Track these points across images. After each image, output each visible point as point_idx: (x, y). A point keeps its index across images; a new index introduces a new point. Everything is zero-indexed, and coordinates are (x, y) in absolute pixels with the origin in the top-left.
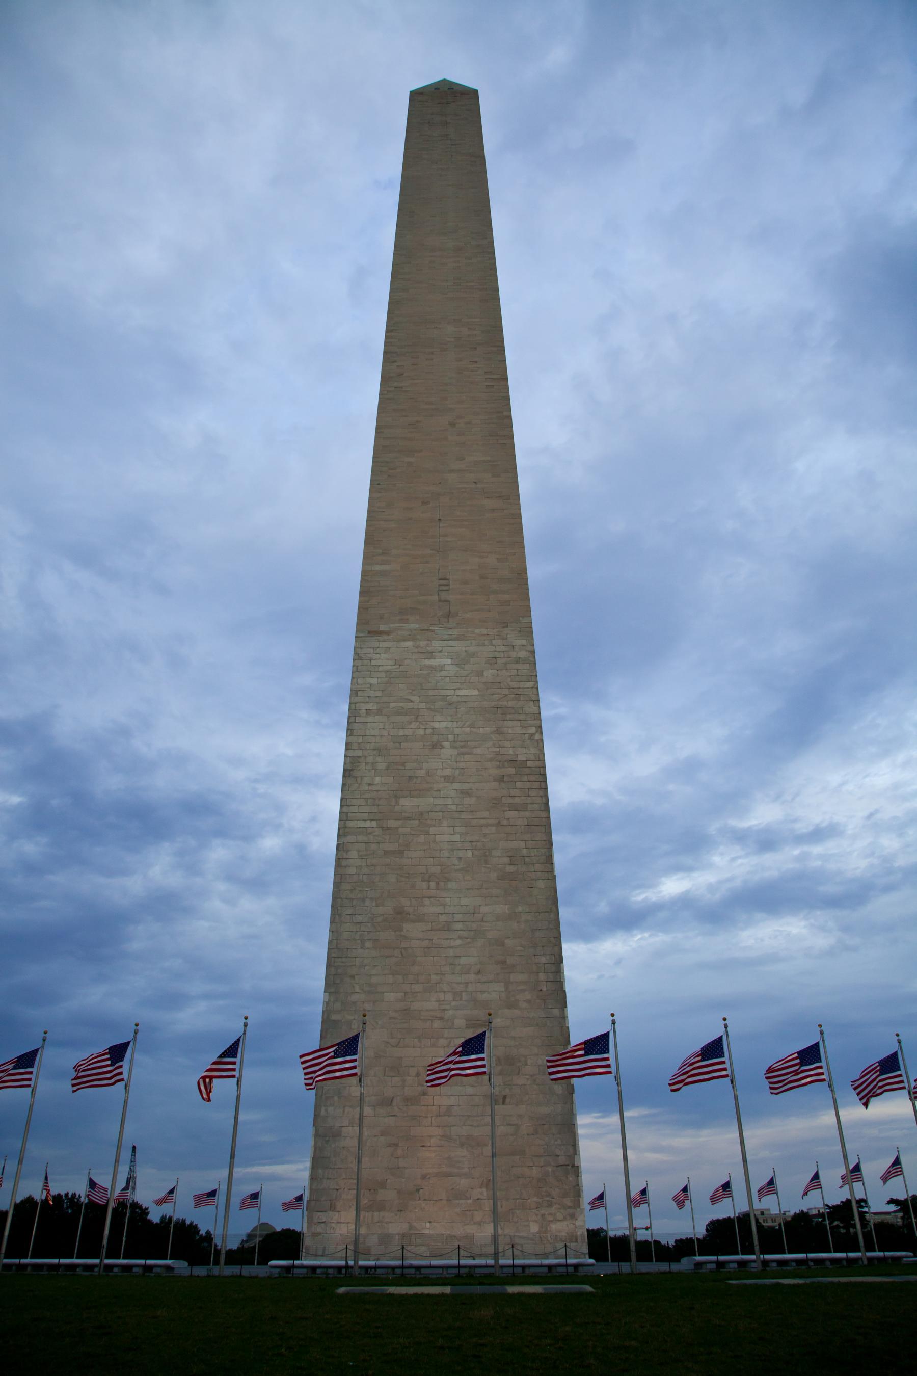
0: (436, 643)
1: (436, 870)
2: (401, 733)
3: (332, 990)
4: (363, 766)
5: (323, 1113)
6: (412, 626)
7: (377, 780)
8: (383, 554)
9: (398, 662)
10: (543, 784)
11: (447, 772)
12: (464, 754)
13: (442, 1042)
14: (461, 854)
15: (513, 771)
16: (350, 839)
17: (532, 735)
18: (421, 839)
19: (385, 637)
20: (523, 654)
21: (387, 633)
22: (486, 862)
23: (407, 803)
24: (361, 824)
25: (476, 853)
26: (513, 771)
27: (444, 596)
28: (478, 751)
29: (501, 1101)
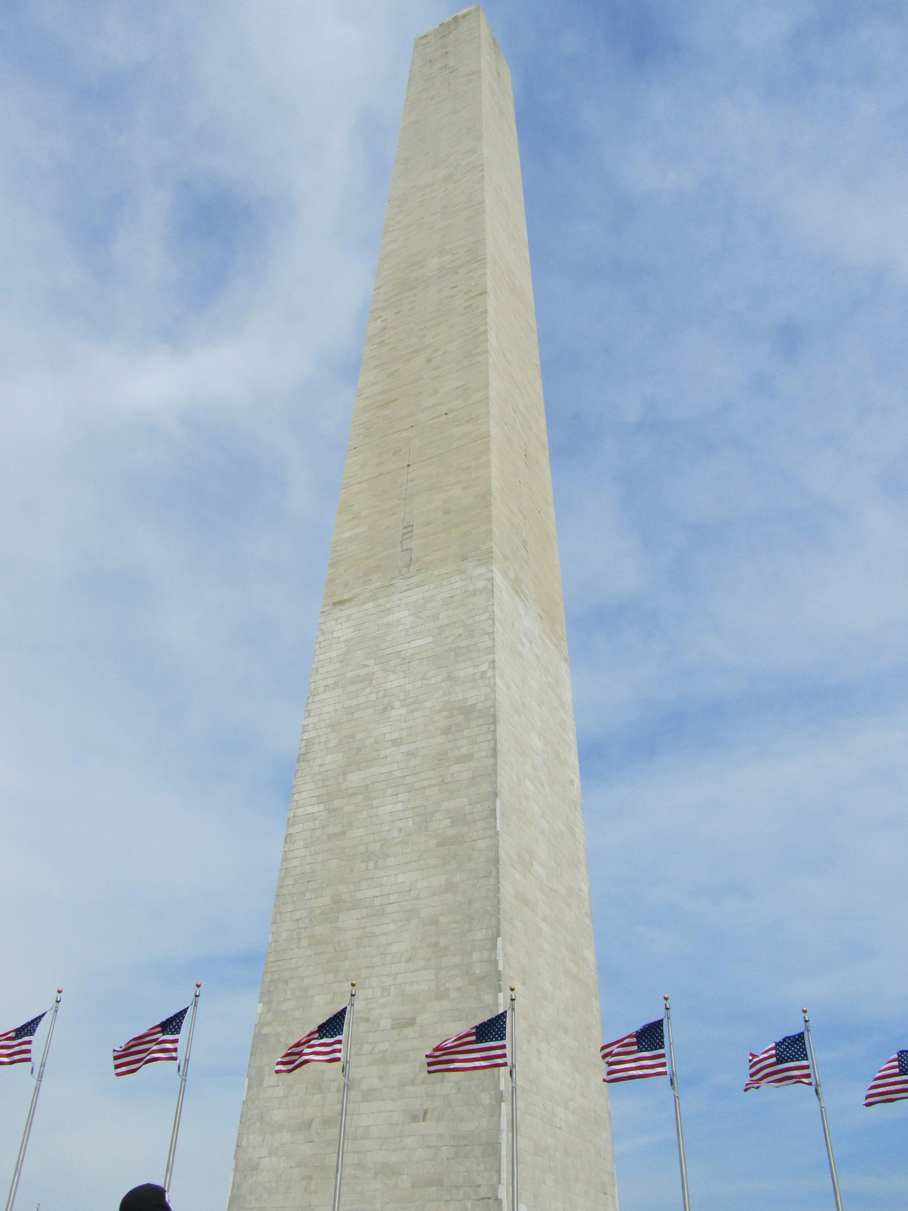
2: (355, 702)
3: (266, 999)
5: (244, 1143)
6: (374, 586)
7: (328, 758)
10: (492, 726)
11: (396, 735)
12: (413, 711)
13: (367, 1048)
14: (401, 824)
15: (461, 718)
17: (484, 672)
18: (364, 815)
19: (348, 605)
21: (350, 600)
22: (426, 830)
23: (355, 778)
24: (310, 809)
25: (417, 819)
27: (407, 544)
28: (428, 704)
29: (421, 1117)
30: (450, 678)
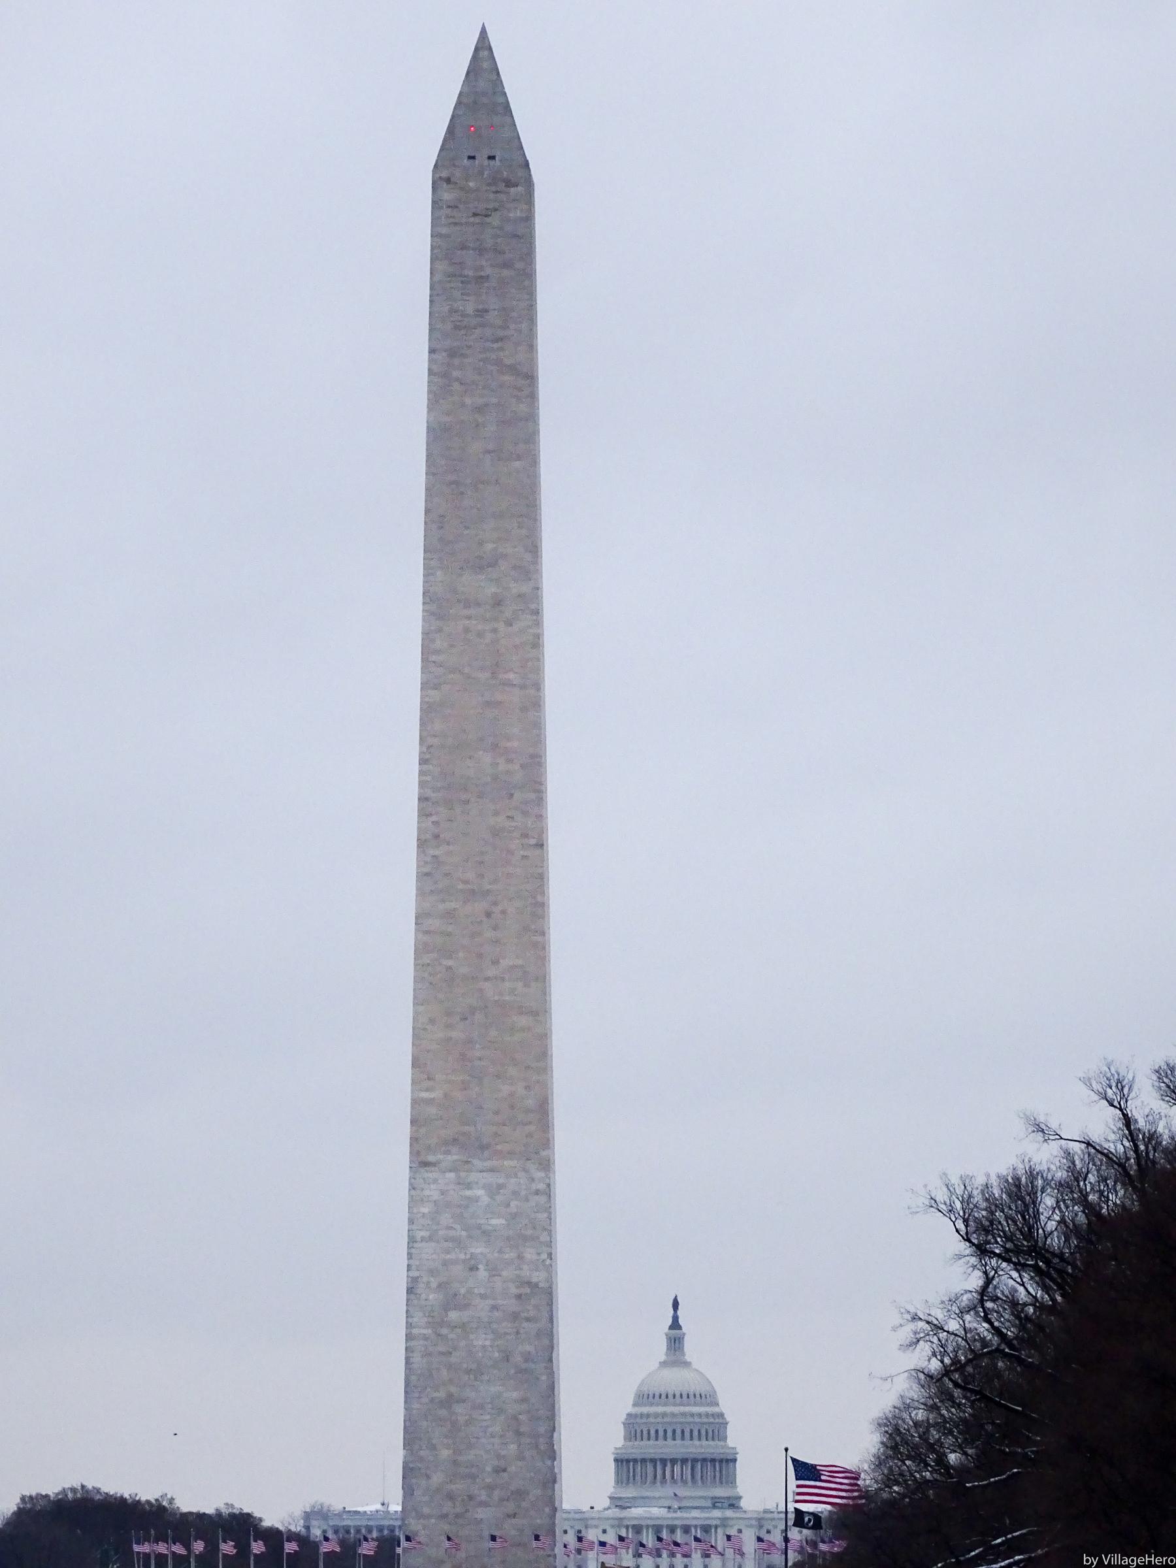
0: (473, 1177)
1: (474, 1366)
4: (421, 1285)
6: (455, 1157)
8: (429, 1079)
9: (443, 1193)
11: (482, 1292)
15: (528, 1291)
16: (412, 1343)
18: (463, 1343)
20: (542, 1186)
23: (453, 1315)
26: (528, 1291)
30: (520, 1257)
